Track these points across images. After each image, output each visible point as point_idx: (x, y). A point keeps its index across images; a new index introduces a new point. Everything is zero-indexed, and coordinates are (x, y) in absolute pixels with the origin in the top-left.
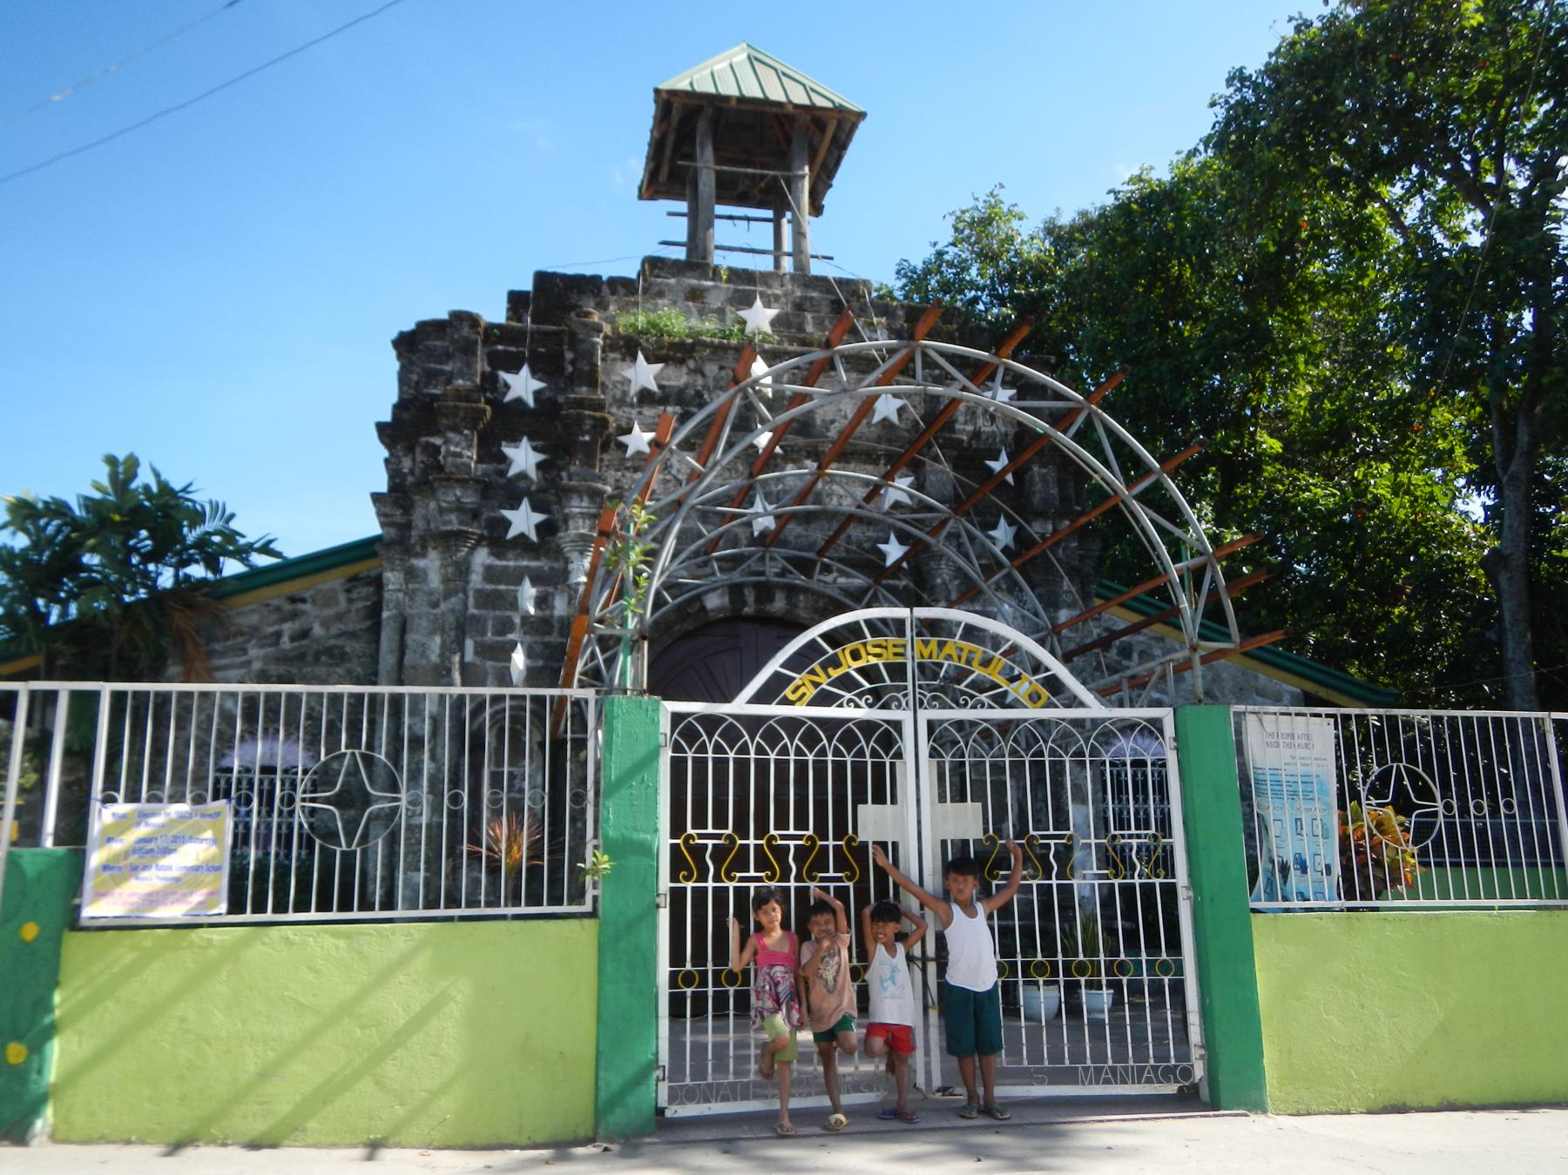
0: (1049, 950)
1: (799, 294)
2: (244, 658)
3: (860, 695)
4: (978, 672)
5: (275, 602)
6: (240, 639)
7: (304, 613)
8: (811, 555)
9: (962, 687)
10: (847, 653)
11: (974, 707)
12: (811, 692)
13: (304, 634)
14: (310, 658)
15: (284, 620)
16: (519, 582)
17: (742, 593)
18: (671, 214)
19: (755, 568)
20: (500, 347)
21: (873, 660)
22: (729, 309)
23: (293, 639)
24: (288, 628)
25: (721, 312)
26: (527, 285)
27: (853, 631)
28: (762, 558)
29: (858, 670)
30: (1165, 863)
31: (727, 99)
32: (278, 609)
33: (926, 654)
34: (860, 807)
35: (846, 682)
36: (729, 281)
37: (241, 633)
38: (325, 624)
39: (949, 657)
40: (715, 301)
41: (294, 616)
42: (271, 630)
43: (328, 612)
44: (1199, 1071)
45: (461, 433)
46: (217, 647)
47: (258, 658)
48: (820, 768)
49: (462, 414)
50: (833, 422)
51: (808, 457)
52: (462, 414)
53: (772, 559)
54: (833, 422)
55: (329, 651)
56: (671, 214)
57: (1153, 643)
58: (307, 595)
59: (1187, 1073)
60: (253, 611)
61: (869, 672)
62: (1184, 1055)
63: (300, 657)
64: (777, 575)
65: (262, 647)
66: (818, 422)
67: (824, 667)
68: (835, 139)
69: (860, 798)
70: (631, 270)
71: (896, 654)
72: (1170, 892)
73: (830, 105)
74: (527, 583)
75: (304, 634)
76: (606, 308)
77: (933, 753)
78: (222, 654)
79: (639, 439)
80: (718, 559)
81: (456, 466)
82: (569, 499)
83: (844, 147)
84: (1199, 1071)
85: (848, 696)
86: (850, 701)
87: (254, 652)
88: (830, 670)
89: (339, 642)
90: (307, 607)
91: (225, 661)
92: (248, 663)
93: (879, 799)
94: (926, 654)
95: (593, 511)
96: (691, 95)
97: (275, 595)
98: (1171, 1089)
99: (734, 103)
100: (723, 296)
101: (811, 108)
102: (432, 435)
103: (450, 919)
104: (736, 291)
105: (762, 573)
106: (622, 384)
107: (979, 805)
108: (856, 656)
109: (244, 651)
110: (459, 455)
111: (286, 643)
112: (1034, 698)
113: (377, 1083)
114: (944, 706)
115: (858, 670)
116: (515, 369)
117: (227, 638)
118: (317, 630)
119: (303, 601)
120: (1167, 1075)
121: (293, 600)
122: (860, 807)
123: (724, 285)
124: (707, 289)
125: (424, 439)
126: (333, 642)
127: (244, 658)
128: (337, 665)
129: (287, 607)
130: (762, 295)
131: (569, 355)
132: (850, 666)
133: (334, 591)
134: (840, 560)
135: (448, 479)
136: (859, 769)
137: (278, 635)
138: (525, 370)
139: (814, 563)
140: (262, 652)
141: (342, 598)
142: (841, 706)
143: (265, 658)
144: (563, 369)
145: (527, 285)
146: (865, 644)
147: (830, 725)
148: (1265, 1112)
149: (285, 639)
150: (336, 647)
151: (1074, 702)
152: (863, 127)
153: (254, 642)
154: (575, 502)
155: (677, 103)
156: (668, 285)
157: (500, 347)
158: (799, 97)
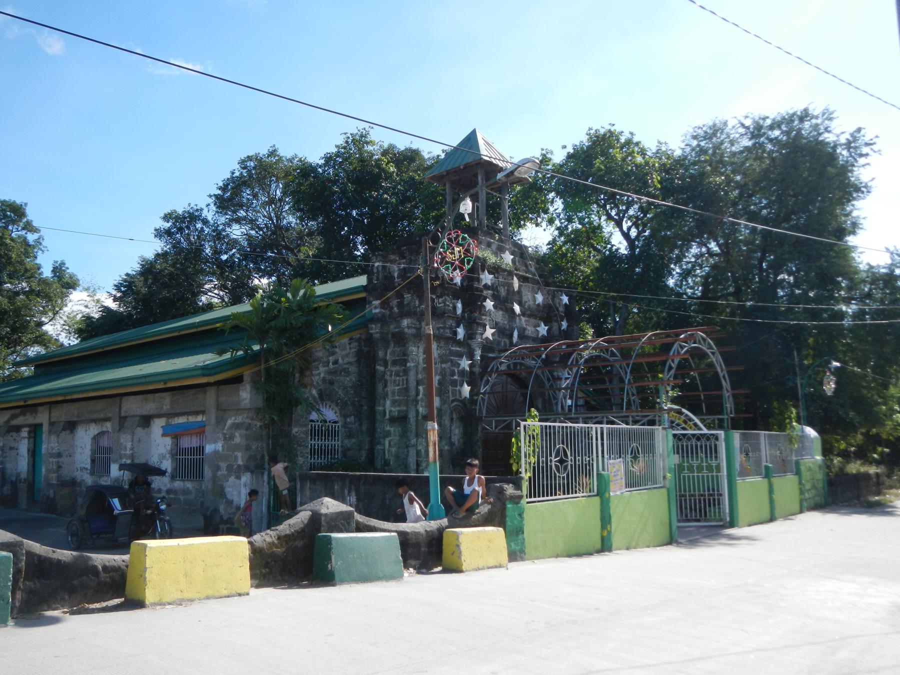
13: (336, 362)
23: (333, 364)
24: (331, 359)
30: (718, 468)
38: (343, 359)
43: (344, 353)
44: (728, 519)
48: (682, 446)
55: (344, 370)
63: (336, 372)
75: (336, 362)
90: (337, 350)
98: (721, 523)
111: (331, 366)
118: (340, 361)
120: (721, 520)
126: (345, 366)
141: (348, 346)
143: (325, 372)
151: (700, 429)
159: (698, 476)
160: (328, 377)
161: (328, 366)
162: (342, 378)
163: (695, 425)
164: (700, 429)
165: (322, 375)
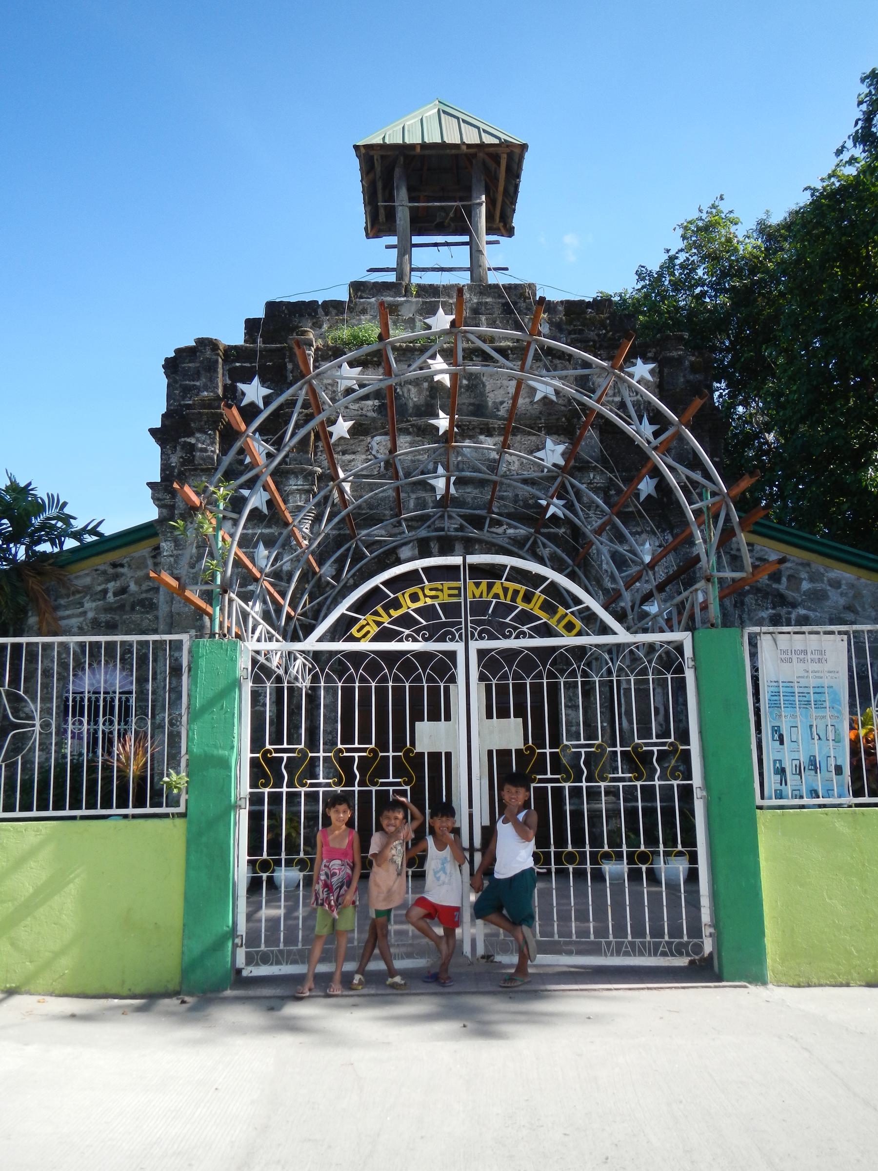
0: (578, 841)
1: (475, 301)
2: (81, 610)
3: (417, 632)
4: (521, 606)
5: (102, 568)
6: (78, 596)
7: (123, 574)
8: (483, 512)
9: (507, 620)
10: (407, 596)
11: (517, 637)
12: (374, 630)
13: (123, 590)
14: (128, 608)
15: (108, 581)
16: (256, 546)
17: (429, 546)
18: (388, 247)
19: (438, 524)
20: (238, 364)
21: (429, 601)
22: (418, 317)
23: (115, 594)
24: (112, 586)
25: (412, 321)
26: (259, 313)
27: (411, 578)
28: (442, 517)
29: (414, 610)
31: (413, 146)
32: (104, 572)
33: (477, 594)
34: (418, 724)
35: (406, 621)
36: (418, 295)
37: (78, 592)
38: (138, 583)
39: (496, 596)
40: (407, 312)
41: (116, 577)
42: (100, 588)
45: (206, 433)
46: (62, 602)
47: (91, 609)
48: (382, 692)
49: (205, 418)
50: (502, 403)
51: (481, 433)
52: (205, 418)
53: (450, 517)
54: (502, 403)
55: (141, 603)
56: (388, 247)
57: (800, 568)
58: (125, 561)
59: (699, 948)
60: (87, 575)
61: (427, 612)
62: (696, 930)
63: (121, 607)
64: (456, 530)
65: (94, 601)
66: (490, 404)
67: (386, 608)
68: (509, 169)
69: (417, 716)
70: (343, 295)
71: (450, 596)
72: (687, 793)
73: (497, 141)
74: (261, 546)
75: (123, 590)
76: (320, 327)
77: (482, 678)
78: (66, 608)
79: (342, 428)
80: (405, 519)
81: (203, 459)
82: (288, 479)
83: (518, 176)
84: (708, 947)
85: (407, 632)
86: (408, 636)
87: (88, 605)
88: (392, 612)
89: (149, 595)
91: (68, 613)
92: (84, 613)
93: (434, 716)
94: (477, 594)
95: (306, 487)
96: (383, 147)
97: (102, 562)
98: (682, 962)
99: (418, 150)
100: (414, 308)
101: (482, 146)
102: (189, 436)
103: (73, 818)
104: (424, 303)
105: (442, 529)
106: (332, 385)
107: (520, 720)
108: (414, 598)
109: (81, 605)
110: (205, 450)
111: (110, 597)
112: (569, 627)
113: (13, 944)
114: (492, 637)
115: (414, 610)
116: (248, 380)
117: (68, 596)
118: (133, 587)
119: (122, 566)
120: (679, 951)
121: (115, 565)
122: (418, 724)
123: (414, 300)
124: (401, 304)
125: (183, 440)
126: (144, 595)
127: (81, 610)
128: (148, 613)
129: (111, 571)
130: (444, 304)
131: (290, 366)
132: (409, 606)
133: (144, 557)
134: (509, 516)
135: (195, 470)
136: (417, 693)
137: (105, 592)
138: (256, 380)
139: (485, 518)
140: (94, 605)
142: (401, 640)
143: (97, 609)
144: (286, 377)
145: (259, 313)
146: (422, 589)
147: (391, 657)
148: (764, 983)
149: (110, 594)
150: (146, 599)
152: (528, 157)
153: (88, 598)
154: (292, 481)
155: (376, 155)
156: (370, 303)
157: (238, 364)
158: (471, 137)
159: (667, 791)
160: (103, 617)
161: (105, 598)
162: (136, 617)
163: (589, 617)
164: (605, 630)
165: (90, 615)
